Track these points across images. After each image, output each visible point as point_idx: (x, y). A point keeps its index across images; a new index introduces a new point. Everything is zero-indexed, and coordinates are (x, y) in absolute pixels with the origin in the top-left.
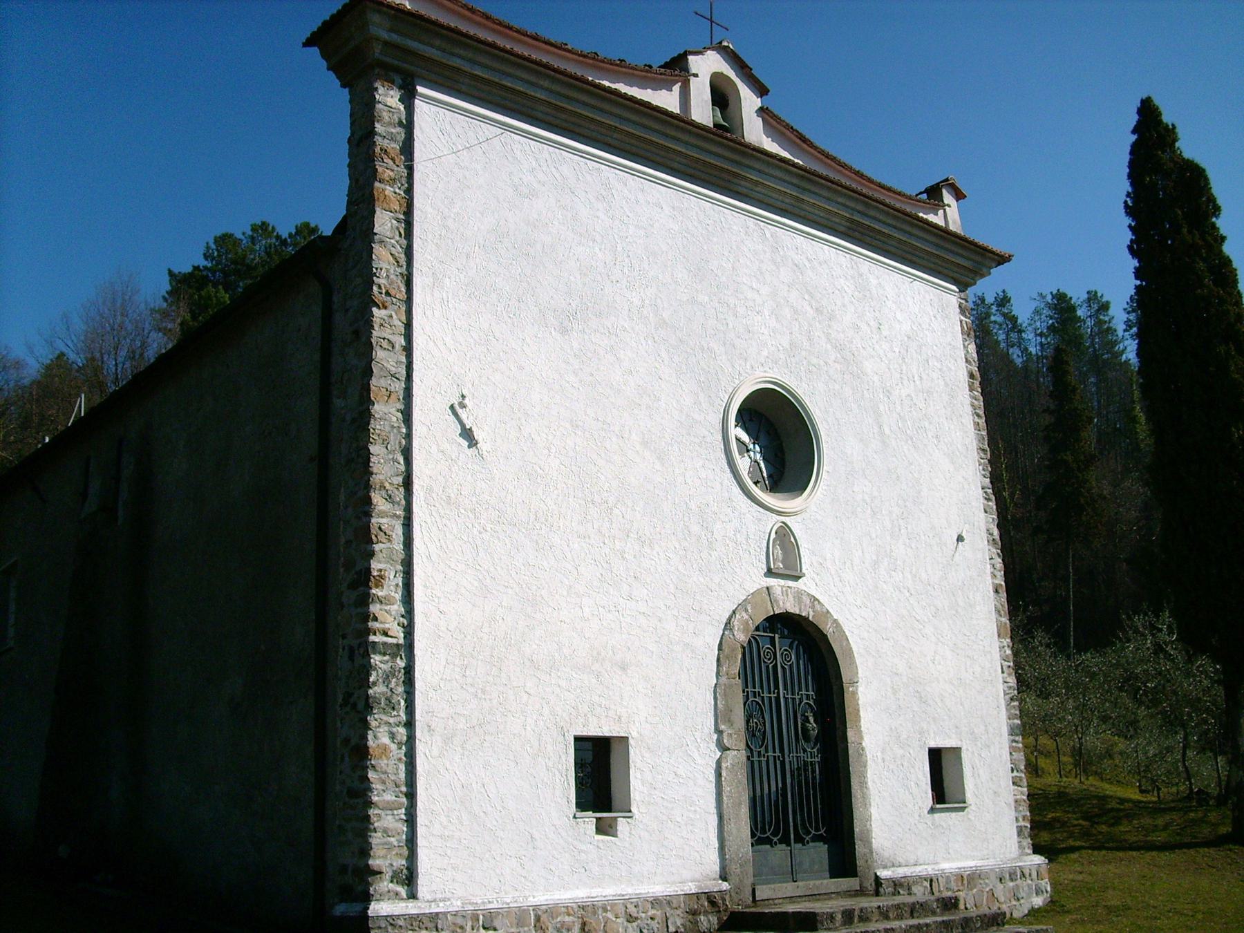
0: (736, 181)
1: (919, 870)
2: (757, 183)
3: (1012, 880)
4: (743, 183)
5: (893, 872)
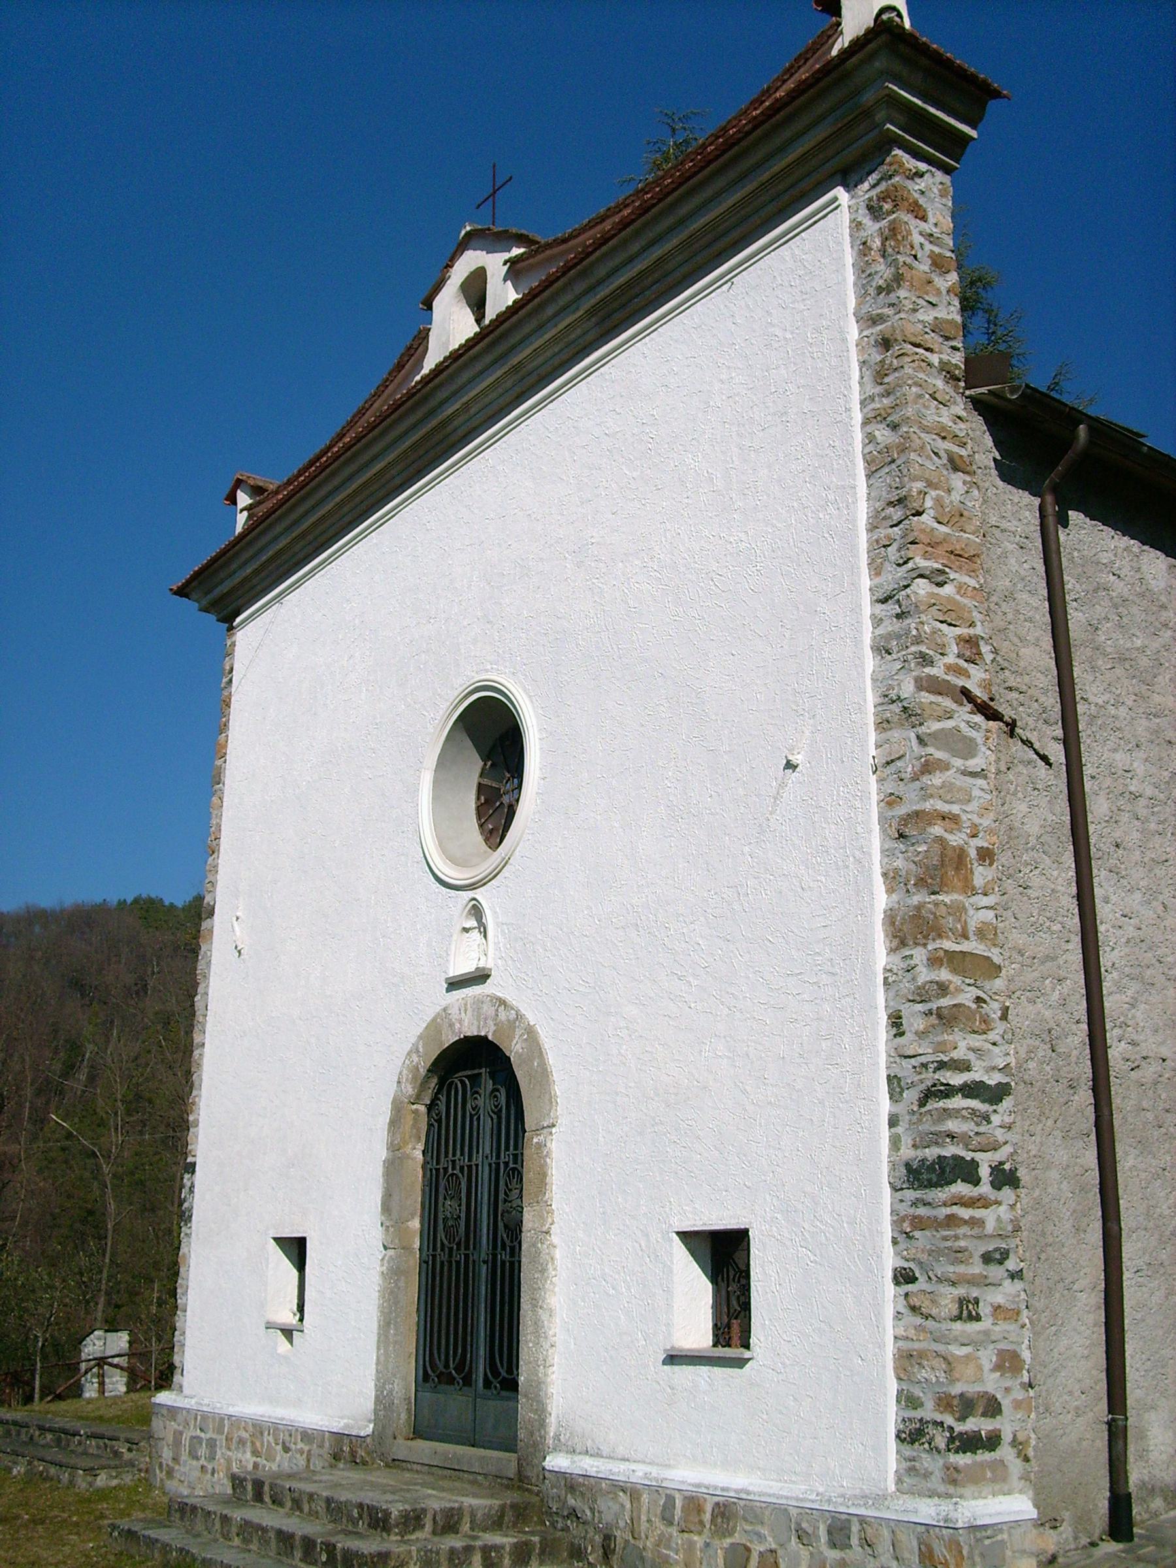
0: (449, 429)
1: (619, 1471)
2: (466, 407)
3: (833, 1545)
4: (456, 423)
5: (573, 1462)
